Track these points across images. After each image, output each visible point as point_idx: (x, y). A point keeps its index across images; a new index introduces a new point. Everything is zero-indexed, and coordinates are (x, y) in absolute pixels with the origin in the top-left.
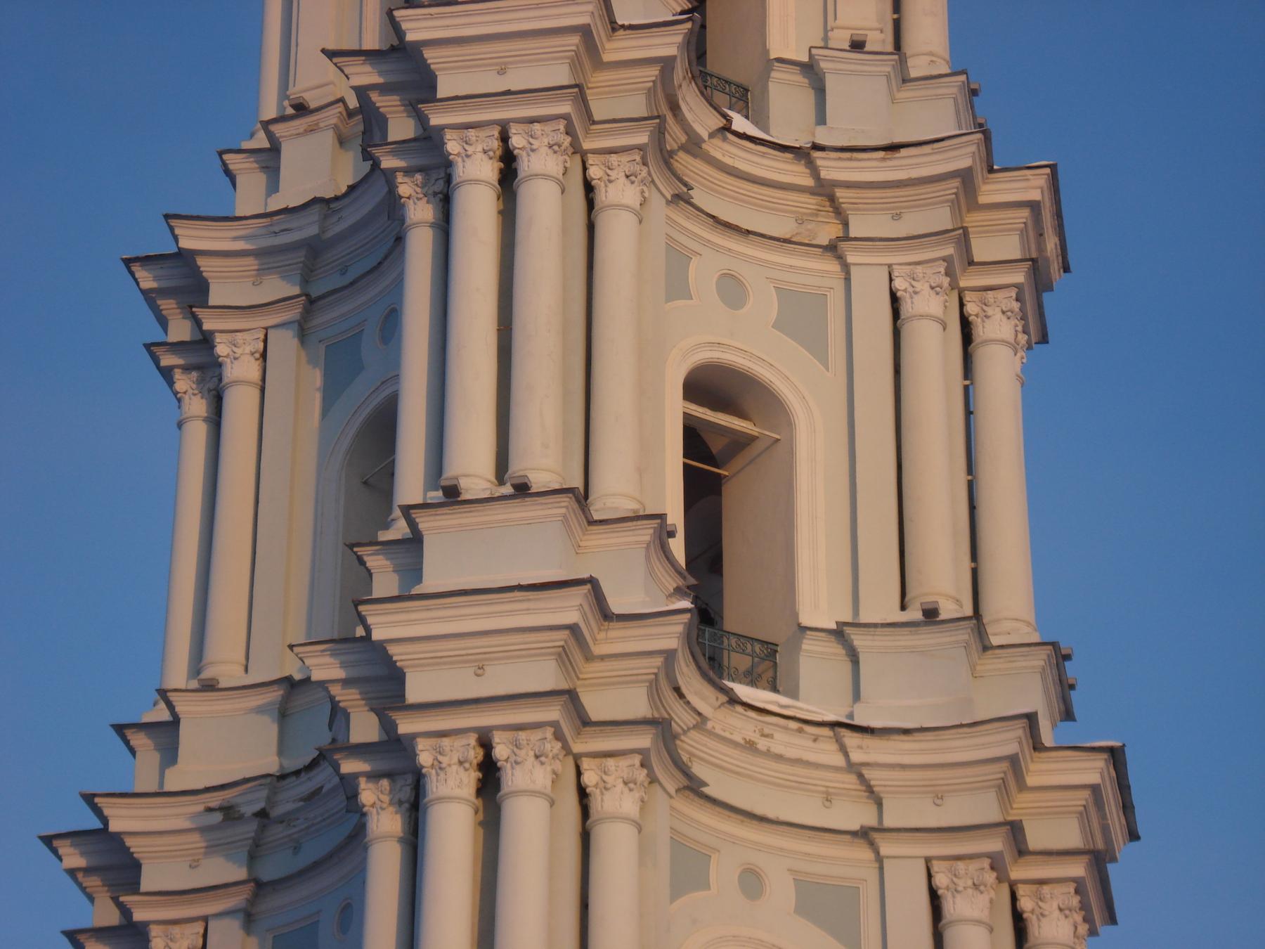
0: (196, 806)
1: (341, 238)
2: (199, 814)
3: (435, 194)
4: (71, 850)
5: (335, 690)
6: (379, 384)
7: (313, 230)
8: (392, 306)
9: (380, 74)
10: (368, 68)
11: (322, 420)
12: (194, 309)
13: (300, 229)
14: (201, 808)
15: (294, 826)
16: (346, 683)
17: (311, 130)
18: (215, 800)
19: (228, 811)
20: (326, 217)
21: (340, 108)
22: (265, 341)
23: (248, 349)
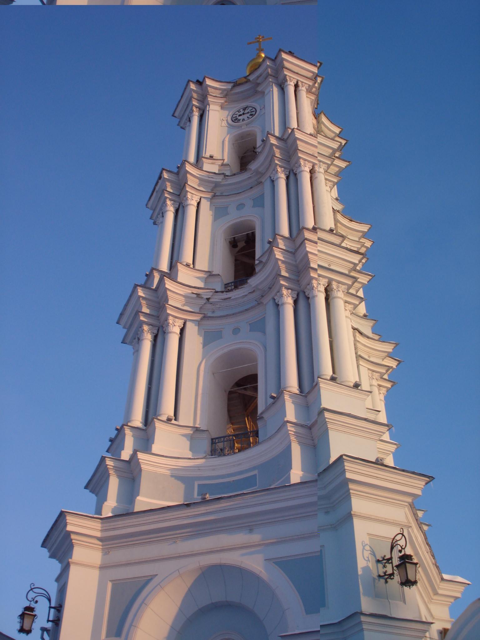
0: (188, 291)
1: (224, 185)
2: (190, 293)
3: (286, 174)
4: (141, 291)
5: (280, 263)
6: (239, 217)
7: (220, 180)
8: (245, 203)
9: (278, 143)
10: (276, 141)
11: (214, 221)
12: (186, 184)
13: (216, 179)
14: (190, 292)
15: (215, 306)
16: (283, 262)
17: (213, 163)
18: (196, 291)
19: (198, 295)
20: (223, 179)
21: (222, 161)
22: (200, 199)
23: (195, 199)
